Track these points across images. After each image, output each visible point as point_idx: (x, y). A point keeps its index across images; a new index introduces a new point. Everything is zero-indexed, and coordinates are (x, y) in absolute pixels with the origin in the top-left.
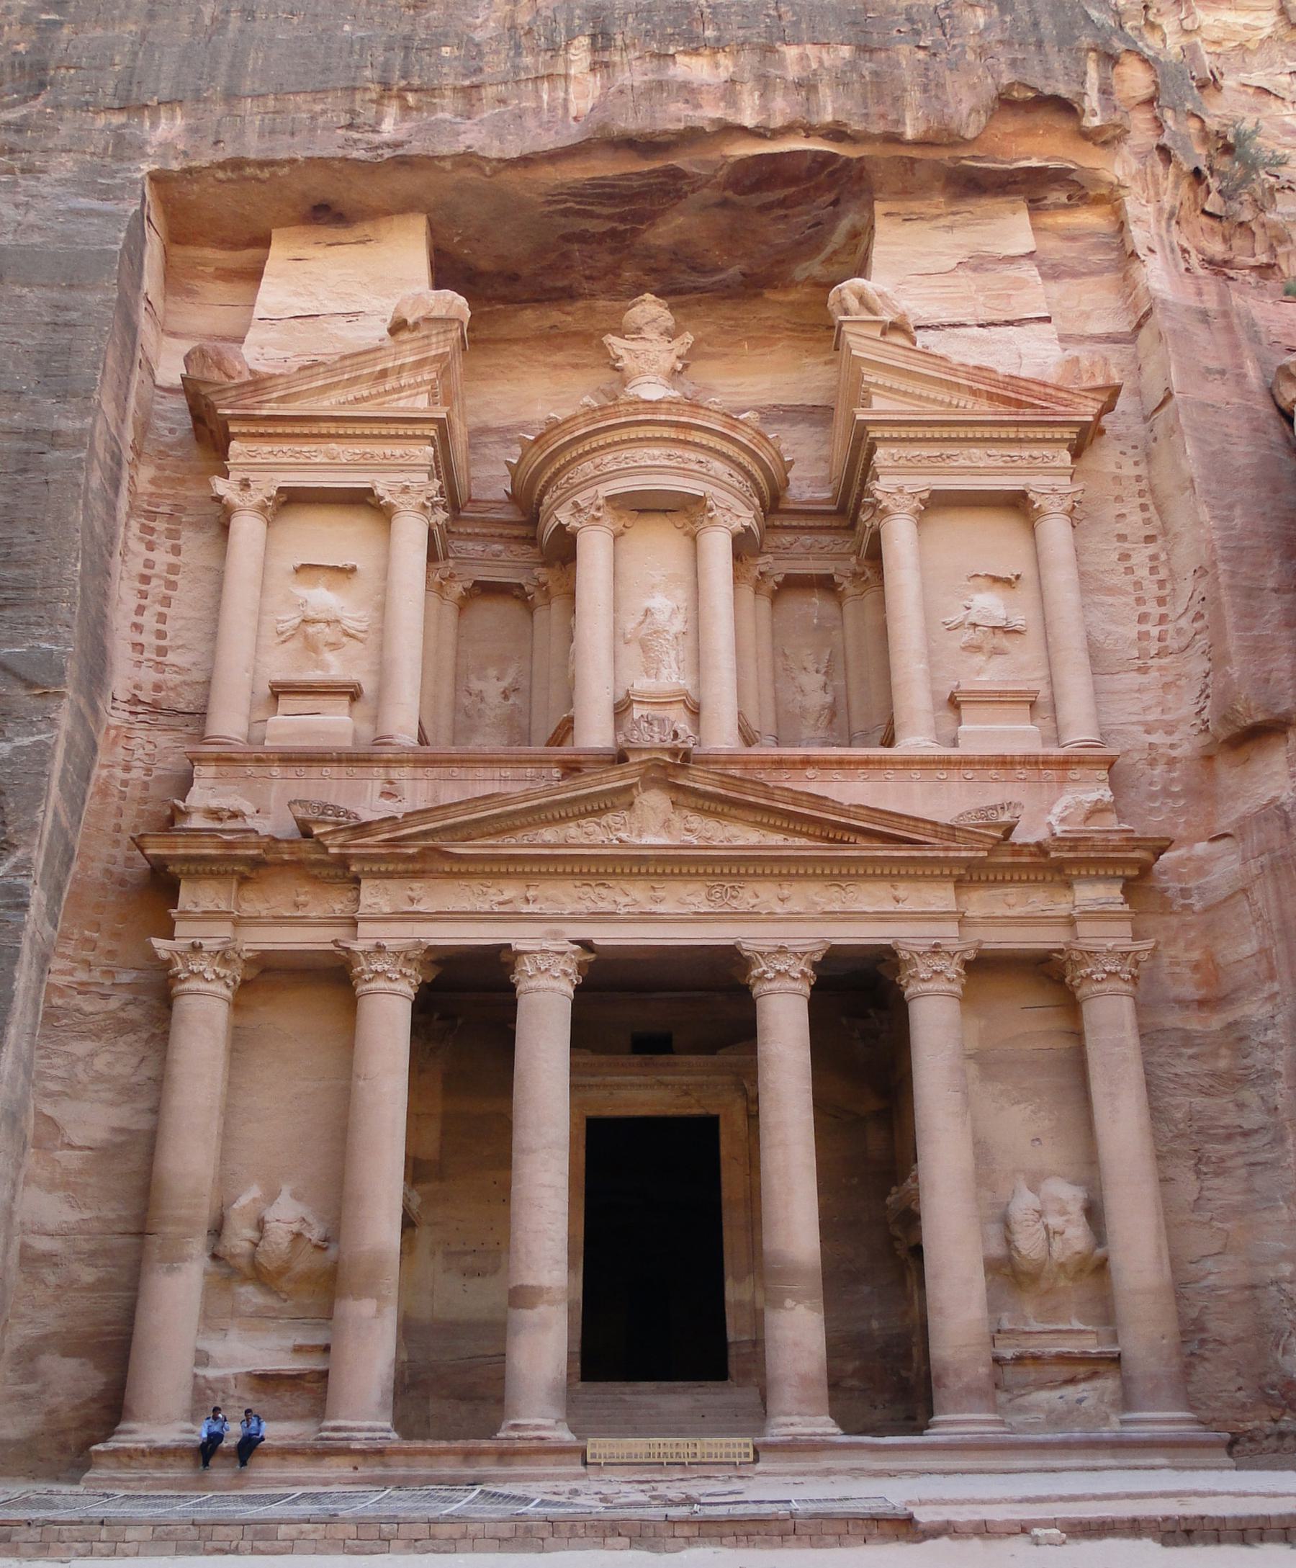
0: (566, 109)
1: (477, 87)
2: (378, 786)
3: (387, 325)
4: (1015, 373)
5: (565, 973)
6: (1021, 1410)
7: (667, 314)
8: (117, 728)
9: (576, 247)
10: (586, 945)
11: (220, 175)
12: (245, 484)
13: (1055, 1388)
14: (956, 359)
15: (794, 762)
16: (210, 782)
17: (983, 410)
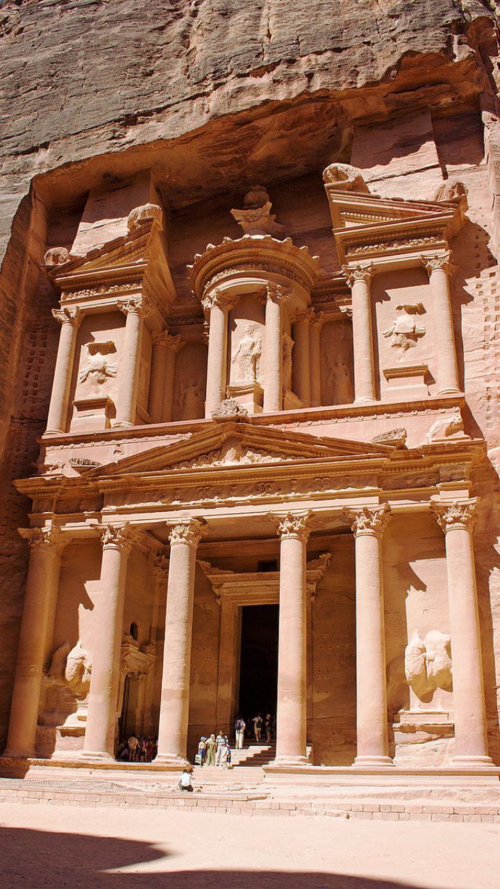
1: (169, 106)
2: (114, 448)
8: (14, 430)
9: (221, 169)
11: (62, 171)
12: (67, 313)
14: (382, 197)
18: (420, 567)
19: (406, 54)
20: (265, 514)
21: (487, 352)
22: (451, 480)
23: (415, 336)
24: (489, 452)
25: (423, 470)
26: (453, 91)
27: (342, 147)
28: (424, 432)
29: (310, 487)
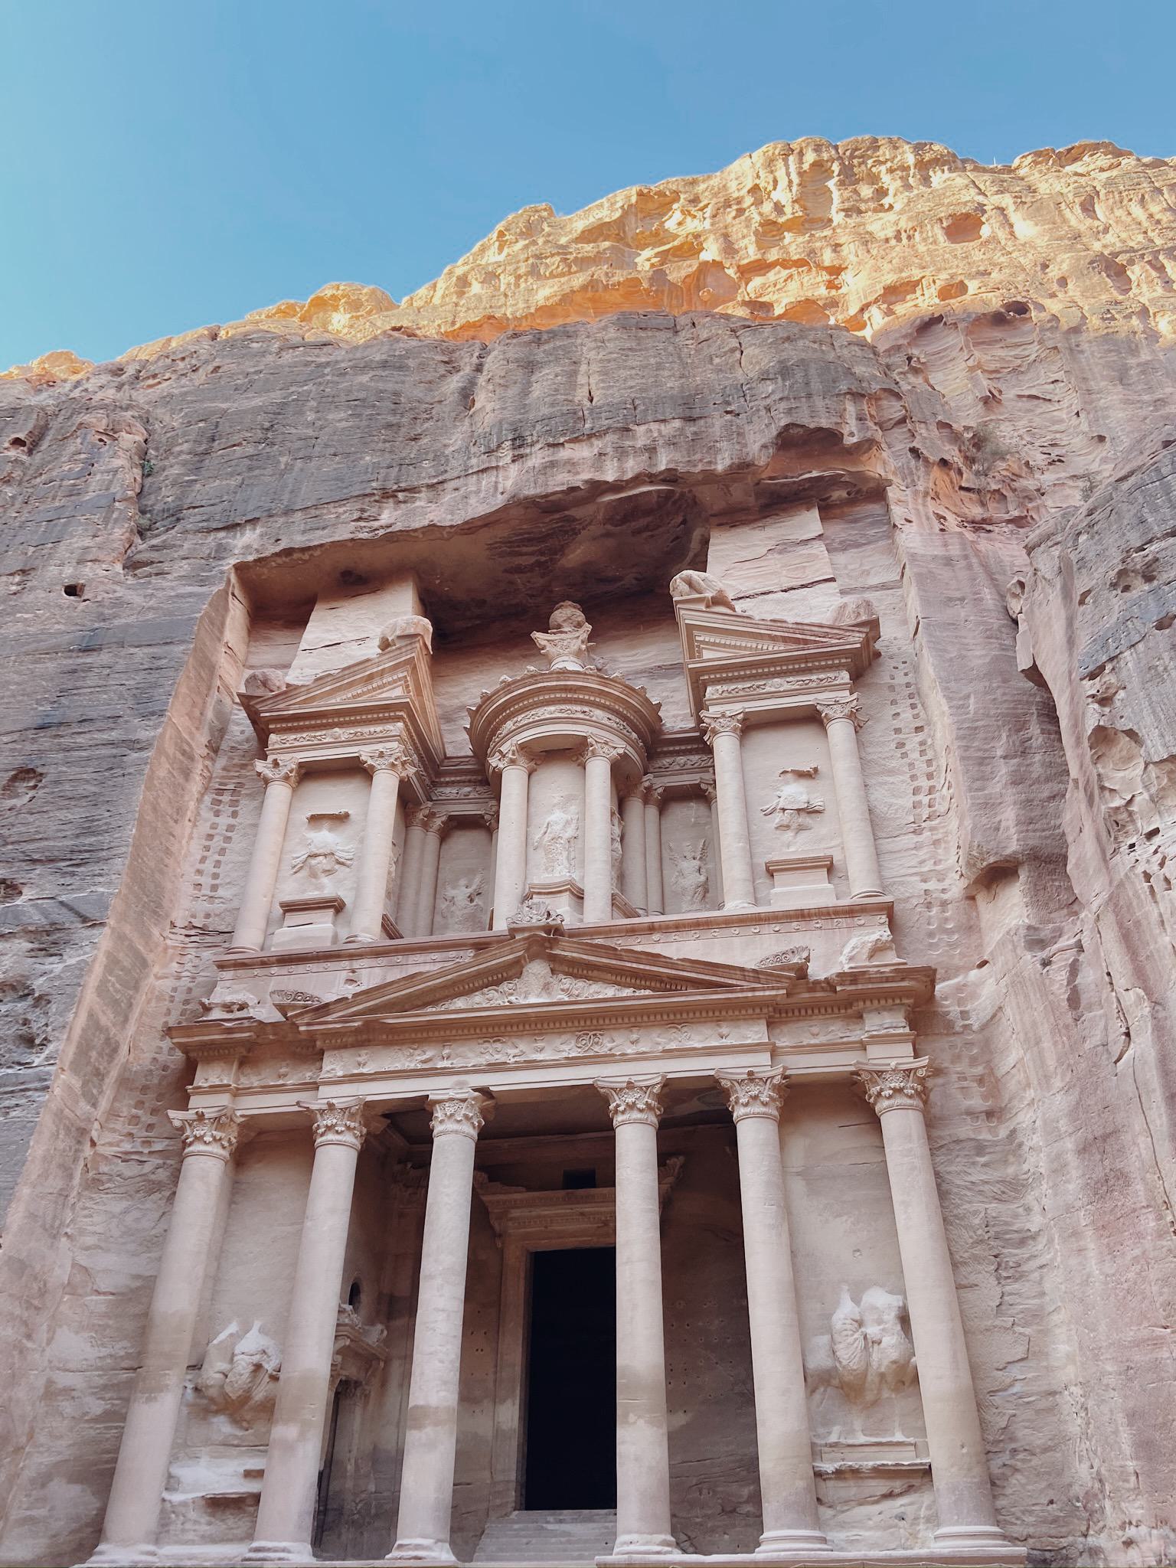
0: (496, 488)
2: (345, 975)
3: (377, 642)
4: (799, 620)
5: (466, 1117)
6: (842, 1526)
7: (579, 613)
10: (485, 1091)
11: (279, 561)
12: (276, 764)
13: (876, 1502)
15: (642, 930)
16: (228, 984)
17: (779, 650)
20: (590, 1082)
21: (920, 838)
24: (937, 987)
27: (691, 554)
28: (834, 954)
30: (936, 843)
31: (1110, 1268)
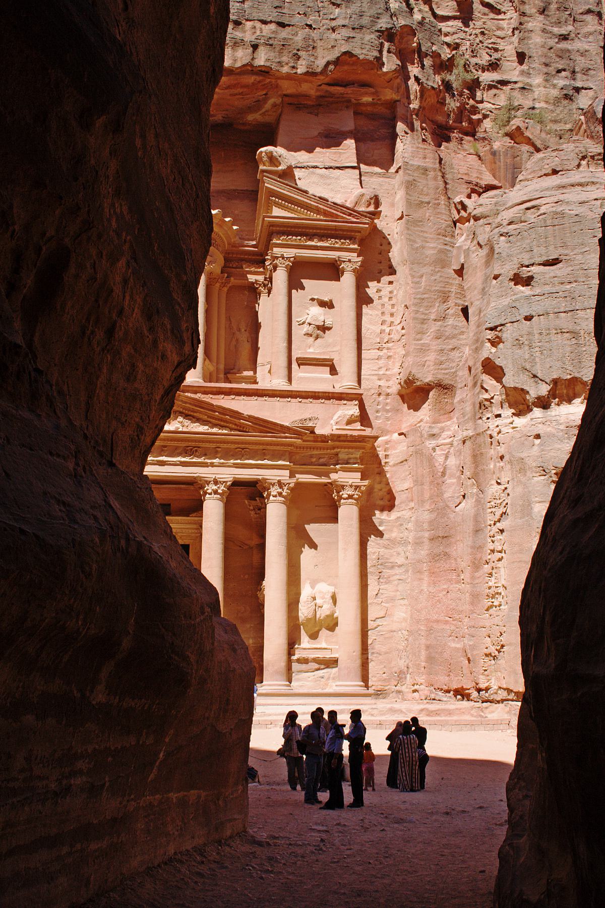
14: (311, 192)
18: (313, 529)
19: (345, 53)
21: (381, 353)
22: (347, 463)
23: (324, 328)
25: (325, 452)
26: (376, 93)
27: (263, 110)
28: (332, 420)
29: (233, 455)
30: (389, 357)
31: (431, 589)
